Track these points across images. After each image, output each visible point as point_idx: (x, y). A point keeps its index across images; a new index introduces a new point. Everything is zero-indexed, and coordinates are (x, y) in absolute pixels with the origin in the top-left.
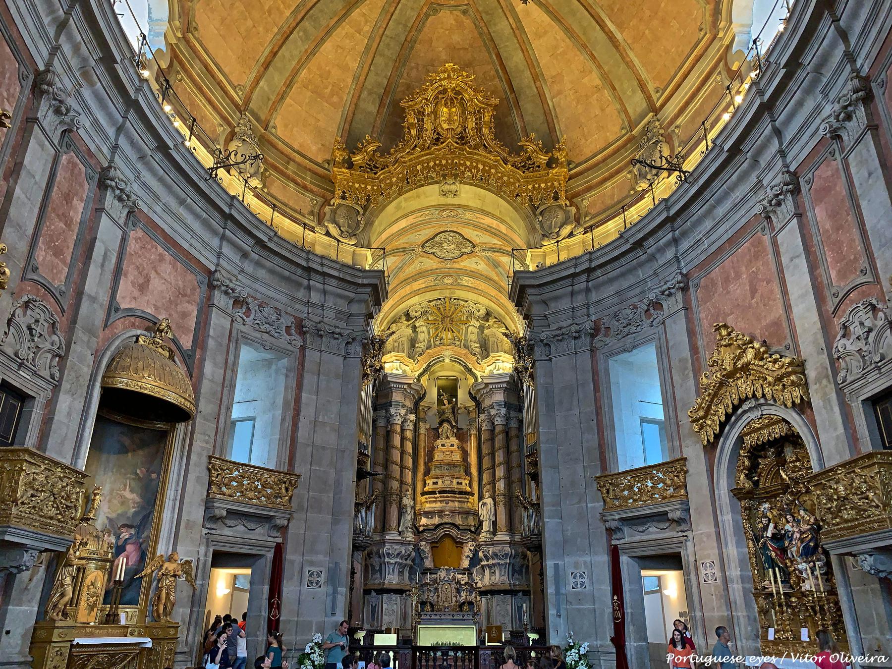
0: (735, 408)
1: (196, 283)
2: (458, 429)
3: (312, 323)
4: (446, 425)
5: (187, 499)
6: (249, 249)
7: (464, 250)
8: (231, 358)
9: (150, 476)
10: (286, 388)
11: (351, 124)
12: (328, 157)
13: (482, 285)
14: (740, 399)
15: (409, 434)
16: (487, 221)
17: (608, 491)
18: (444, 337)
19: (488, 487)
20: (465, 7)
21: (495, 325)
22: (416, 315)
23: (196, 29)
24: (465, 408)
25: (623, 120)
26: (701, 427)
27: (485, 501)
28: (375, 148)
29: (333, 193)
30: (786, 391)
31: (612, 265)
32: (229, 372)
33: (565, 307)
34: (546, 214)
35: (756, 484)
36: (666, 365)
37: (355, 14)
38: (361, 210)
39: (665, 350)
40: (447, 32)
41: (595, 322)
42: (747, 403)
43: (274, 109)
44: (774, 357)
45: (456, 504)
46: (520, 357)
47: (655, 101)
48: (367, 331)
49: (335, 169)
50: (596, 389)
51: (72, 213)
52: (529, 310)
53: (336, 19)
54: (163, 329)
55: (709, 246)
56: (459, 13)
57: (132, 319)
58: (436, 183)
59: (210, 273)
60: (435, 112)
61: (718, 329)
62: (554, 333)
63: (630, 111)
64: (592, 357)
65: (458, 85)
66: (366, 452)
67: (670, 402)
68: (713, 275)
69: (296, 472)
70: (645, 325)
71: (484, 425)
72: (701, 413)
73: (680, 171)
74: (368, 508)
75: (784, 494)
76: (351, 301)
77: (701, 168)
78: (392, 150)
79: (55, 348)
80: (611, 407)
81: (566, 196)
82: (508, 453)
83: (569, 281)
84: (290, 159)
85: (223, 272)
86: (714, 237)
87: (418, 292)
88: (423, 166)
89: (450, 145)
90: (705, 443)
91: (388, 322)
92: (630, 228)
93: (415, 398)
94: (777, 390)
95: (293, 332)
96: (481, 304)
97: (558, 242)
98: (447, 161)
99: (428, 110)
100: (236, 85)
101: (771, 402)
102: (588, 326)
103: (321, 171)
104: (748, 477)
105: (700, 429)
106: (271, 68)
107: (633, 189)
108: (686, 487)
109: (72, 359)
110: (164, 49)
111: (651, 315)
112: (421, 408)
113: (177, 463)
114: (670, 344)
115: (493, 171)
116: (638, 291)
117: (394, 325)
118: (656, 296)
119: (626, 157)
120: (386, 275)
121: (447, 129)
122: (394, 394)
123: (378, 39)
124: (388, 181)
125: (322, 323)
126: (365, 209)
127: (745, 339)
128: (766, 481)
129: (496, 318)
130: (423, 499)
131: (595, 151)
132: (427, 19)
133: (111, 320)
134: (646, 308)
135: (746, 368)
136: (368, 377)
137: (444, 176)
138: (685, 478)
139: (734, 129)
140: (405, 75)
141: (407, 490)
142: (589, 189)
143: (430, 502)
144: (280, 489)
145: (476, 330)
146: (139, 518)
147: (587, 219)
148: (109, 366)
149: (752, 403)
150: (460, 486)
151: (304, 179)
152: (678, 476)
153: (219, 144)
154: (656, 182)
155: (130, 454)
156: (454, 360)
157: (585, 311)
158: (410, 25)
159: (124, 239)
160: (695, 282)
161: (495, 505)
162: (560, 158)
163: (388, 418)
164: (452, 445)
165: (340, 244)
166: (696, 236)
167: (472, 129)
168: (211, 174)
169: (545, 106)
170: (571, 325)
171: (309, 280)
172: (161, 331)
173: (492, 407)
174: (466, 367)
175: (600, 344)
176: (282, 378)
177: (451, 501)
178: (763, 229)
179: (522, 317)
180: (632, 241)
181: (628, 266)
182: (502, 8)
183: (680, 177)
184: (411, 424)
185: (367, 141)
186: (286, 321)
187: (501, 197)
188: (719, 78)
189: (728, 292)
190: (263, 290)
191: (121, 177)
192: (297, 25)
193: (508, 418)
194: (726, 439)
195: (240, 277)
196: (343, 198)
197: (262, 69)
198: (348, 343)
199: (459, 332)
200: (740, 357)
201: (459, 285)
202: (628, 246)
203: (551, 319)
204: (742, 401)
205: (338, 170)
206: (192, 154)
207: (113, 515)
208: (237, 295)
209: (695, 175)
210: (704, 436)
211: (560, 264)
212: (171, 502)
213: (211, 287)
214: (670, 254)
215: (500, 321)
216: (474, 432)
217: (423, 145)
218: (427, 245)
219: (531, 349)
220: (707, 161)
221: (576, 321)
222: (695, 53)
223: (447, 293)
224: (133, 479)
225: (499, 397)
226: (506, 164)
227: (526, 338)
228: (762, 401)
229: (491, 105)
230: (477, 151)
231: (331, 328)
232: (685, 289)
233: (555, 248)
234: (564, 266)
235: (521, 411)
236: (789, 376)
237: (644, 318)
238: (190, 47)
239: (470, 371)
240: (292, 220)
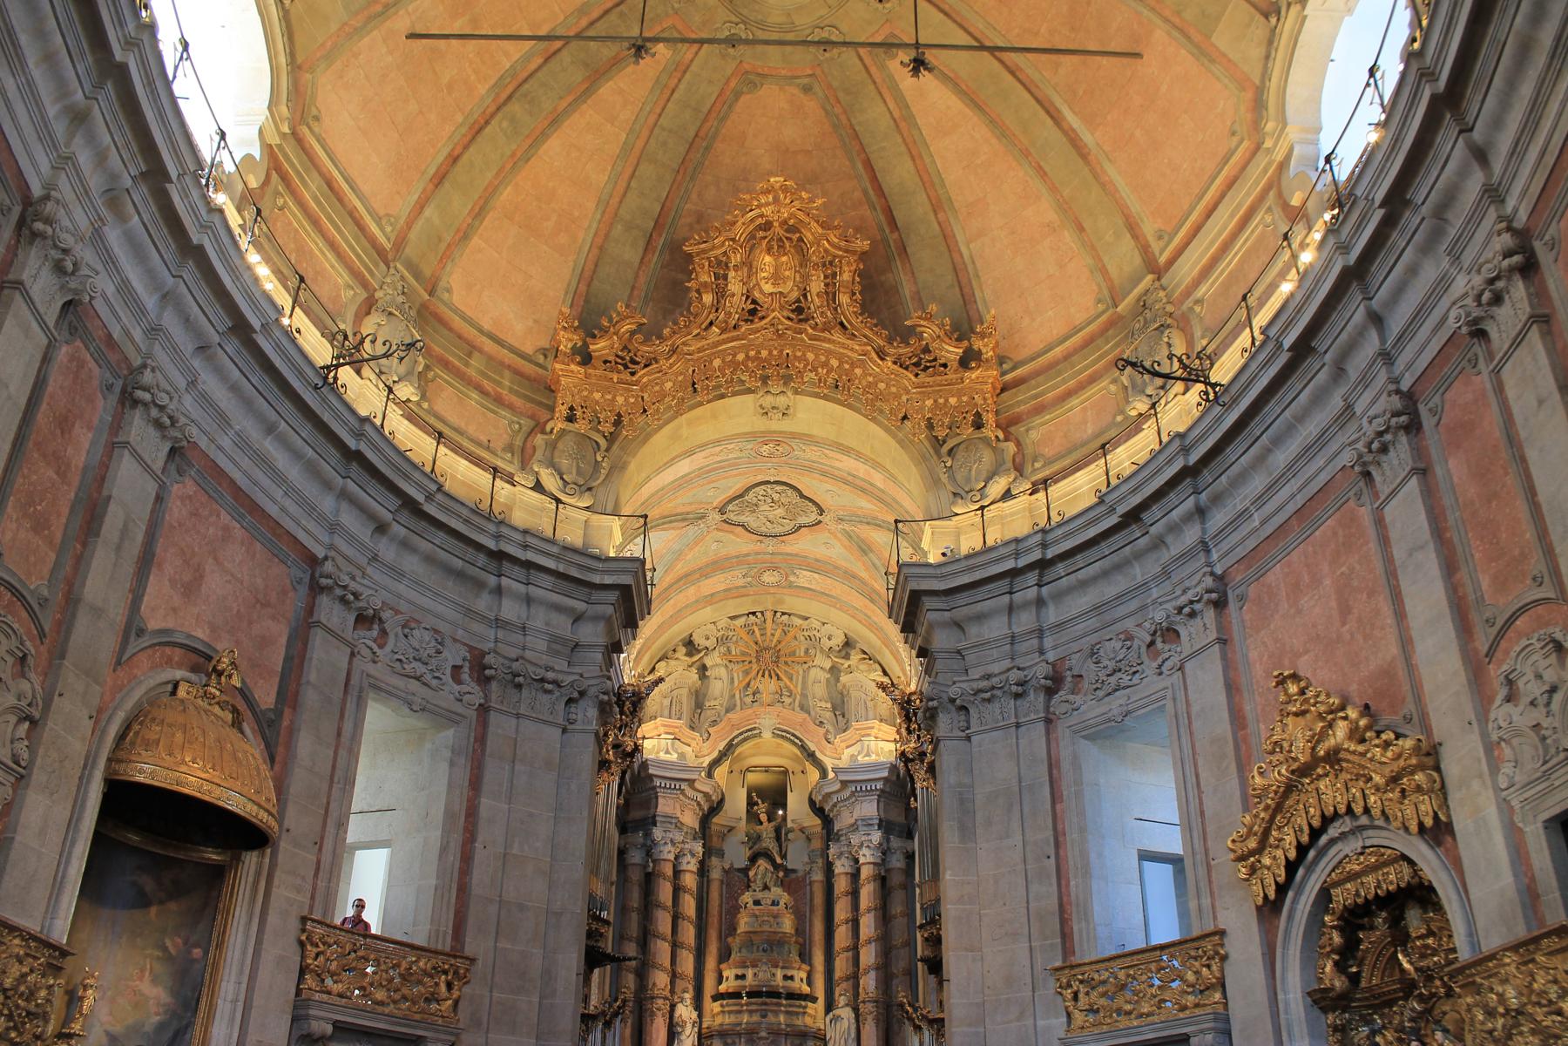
0: (1315, 834)
1: (288, 581)
2: (787, 871)
3: (501, 660)
4: (762, 863)
5: (257, 1001)
6: (388, 516)
7: (803, 520)
8: (348, 727)
9: (190, 953)
10: (450, 786)
12: (544, 342)
13: (838, 588)
14: (1323, 816)
15: (689, 880)
16: (847, 464)
17: (1076, 997)
18: (761, 687)
19: (844, 985)
20: (806, 81)
21: (862, 667)
22: (708, 643)
23: (317, 118)
24: (802, 830)
25: (1099, 285)
26: (1253, 870)
27: (836, 1012)
28: (634, 327)
29: (552, 409)
30: (1406, 802)
31: (1086, 553)
32: (343, 753)
33: (995, 634)
34: (960, 454)
35: (1355, 979)
36: (1187, 751)
37: (606, 90)
38: (603, 443)
39: (1184, 721)
41: (1054, 665)
42: (1336, 824)
43: (446, 257)
44: (1384, 736)
45: (782, 1018)
46: (909, 731)
47: (1157, 254)
48: (610, 678)
49: (558, 366)
50: (1055, 798)
51: (70, 451)
52: (927, 640)
53: (570, 99)
54: (224, 671)
55: (1263, 523)
56: (796, 91)
57: (168, 650)
58: (749, 391)
59: (313, 561)
60: (748, 264)
61: (1281, 681)
62: (975, 685)
63: (1113, 271)
64: (1048, 733)
65: (792, 216)
66: (604, 915)
67: (1194, 818)
68: (1271, 578)
69: (469, 950)
70: (1148, 672)
72: (1252, 844)
73: (1206, 383)
74: (608, 1024)
75: (1406, 998)
76: (578, 618)
77: (1243, 378)
78: (666, 331)
79: (24, 703)
80: (1082, 830)
81: (996, 421)
82: (884, 916)
83: (1003, 585)
84: (472, 348)
85: (340, 560)
86: (1269, 508)
87: (711, 599)
90: (1260, 901)
91: (651, 658)
92: (1117, 487)
93: (701, 808)
94: (1391, 800)
95: (465, 676)
96: (834, 624)
97: (982, 508)
98: (770, 353)
99: (736, 259)
100: (382, 212)
101: (1381, 822)
102: (1042, 670)
103: (529, 368)
104: (1340, 967)
105: (1251, 875)
106: (447, 184)
107: (1122, 412)
108: (1223, 986)
109: (53, 726)
110: (258, 158)
111: (1158, 654)
112: (713, 827)
113: (241, 929)
114: (1195, 709)
115: (858, 371)
116: (1133, 605)
117: (662, 664)
118: (1168, 616)
119: (1107, 353)
120: (648, 566)
121: (771, 294)
122: (661, 801)
123: (645, 133)
124: (657, 388)
125: (521, 661)
126: (611, 438)
127: (1331, 701)
128: (1372, 975)
129: (865, 653)
130: (716, 1007)
133: (130, 651)
134: (1148, 639)
135: (1333, 757)
136: (610, 768)
137: (765, 380)
138: (1222, 970)
139: (1299, 310)
140: (694, 196)
142: (1040, 410)
143: (730, 1012)
144: (437, 984)
145: (824, 676)
146: (169, 1034)
147: (1037, 465)
148: (122, 737)
149: (1345, 825)
151: (499, 384)
152: (1208, 966)
153: (344, 322)
154: (1163, 401)
155: (153, 910)
156: (781, 734)
157: (1035, 642)
158: (705, 110)
159: (159, 499)
160: (1238, 591)
161: (857, 1021)
162: (984, 351)
163: (649, 849)
164: (774, 903)
165: (561, 506)
166: (1237, 503)
167: (818, 295)
168: (325, 379)
170: (1009, 670)
171: (499, 576)
172: (220, 674)
173: (854, 827)
174: (803, 748)
175: (1064, 707)
176: (444, 766)
177: (772, 1011)
178: (1359, 496)
179: (914, 653)
180: (1122, 509)
181: (1115, 558)
182: (874, 82)
183: (1206, 393)
184: (693, 861)
185: (618, 314)
186: (454, 655)
187: (874, 420)
188: (1268, 219)
189: (1299, 612)
190: (413, 595)
191: (164, 385)
192: (498, 109)
193: (885, 851)
194: (1298, 893)
195: (369, 570)
196: (571, 419)
197: (431, 186)
198: (570, 701)
199: (791, 679)
200: (1322, 736)
201: (791, 586)
202: (1113, 520)
203: (971, 658)
204: (1327, 821)
205: (563, 367)
206: (293, 341)
207: (117, 1029)
208: (361, 604)
209: (1233, 390)
210: (1257, 889)
211: (987, 550)
212: (228, 1005)
213: (316, 589)
214: (1191, 535)
215: (868, 656)
216: (818, 876)
217: (726, 322)
218: (730, 507)
219: (932, 715)
220: (1254, 366)
221: (1020, 662)
222: (1224, 173)
223: (768, 604)
224: (158, 958)
225: (869, 808)
226: (882, 359)
227: (921, 693)
228: (1364, 820)
229: (854, 253)
230: (826, 335)
231: (538, 671)
232: (1220, 605)
233: (978, 519)
234: (994, 555)
235: (910, 836)
236: (1412, 773)
237: (1144, 657)
238: (303, 149)
239: (811, 756)
240: (471, 461)
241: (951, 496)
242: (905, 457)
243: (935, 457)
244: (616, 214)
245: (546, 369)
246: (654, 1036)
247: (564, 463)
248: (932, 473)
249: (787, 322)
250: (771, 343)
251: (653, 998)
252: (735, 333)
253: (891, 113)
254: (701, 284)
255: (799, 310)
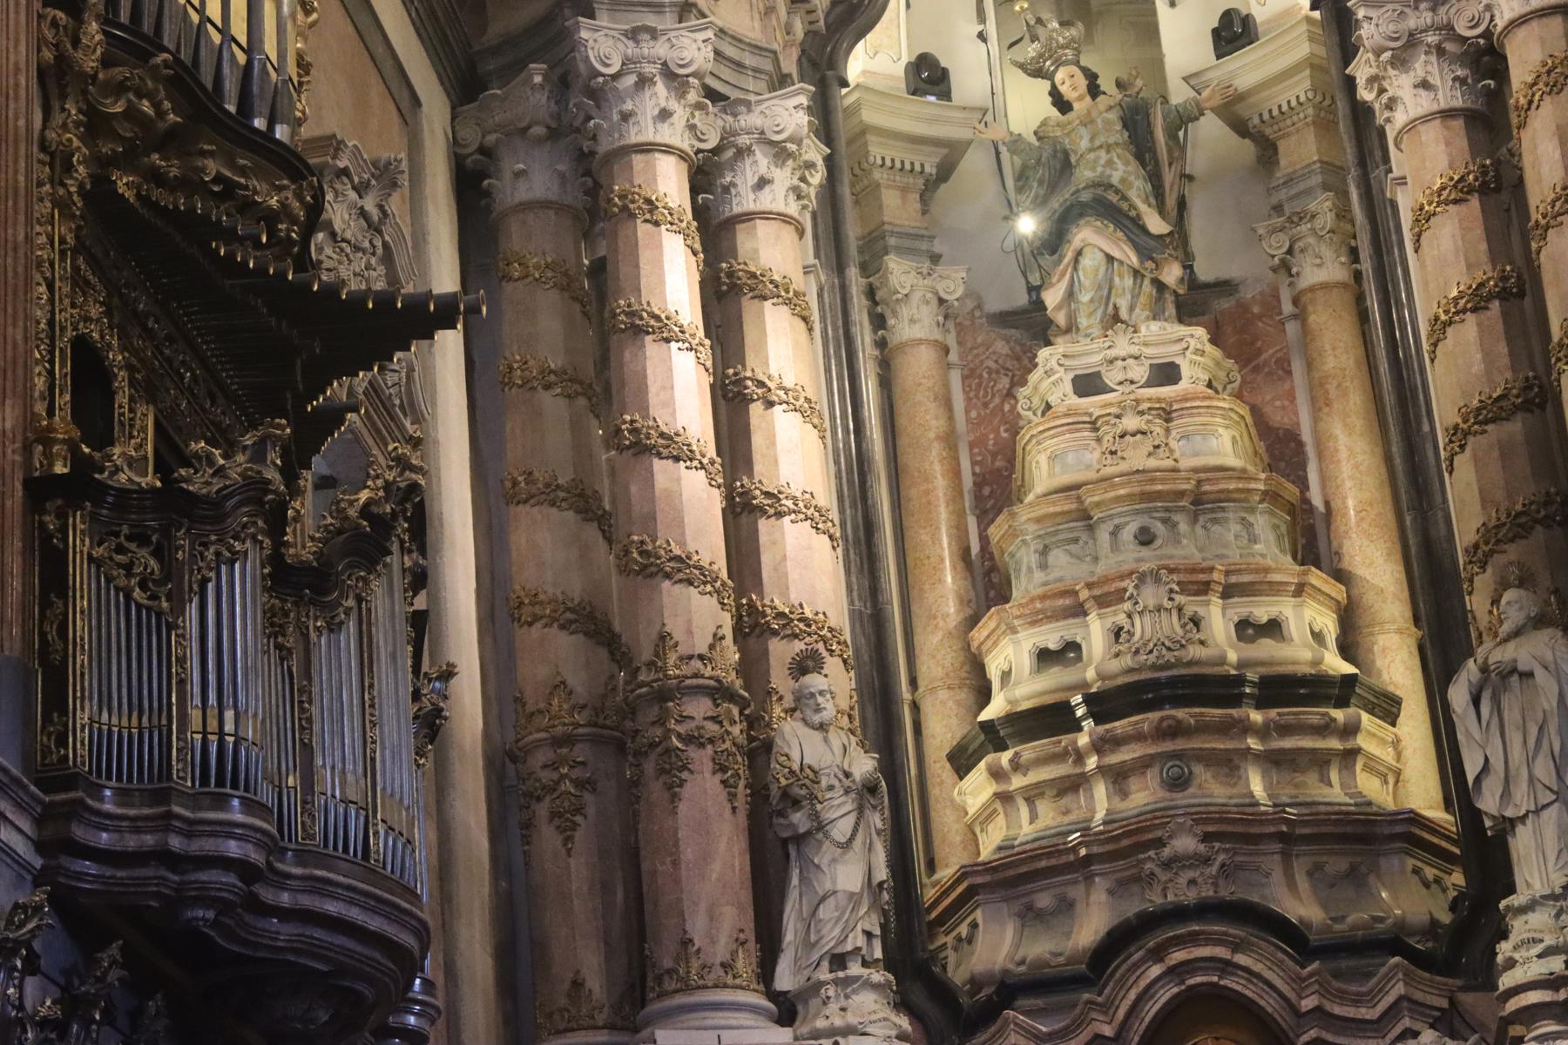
24: (1235, 113)
71: (1401, 84)
112: (877, 150)
130: (976, 789)
141: (805, 665)
143: (1032, 795)
150: (1266, 648)
164: (1167, 373)
184: (783, 178)
246: (688, 853)
251: (663, 696)
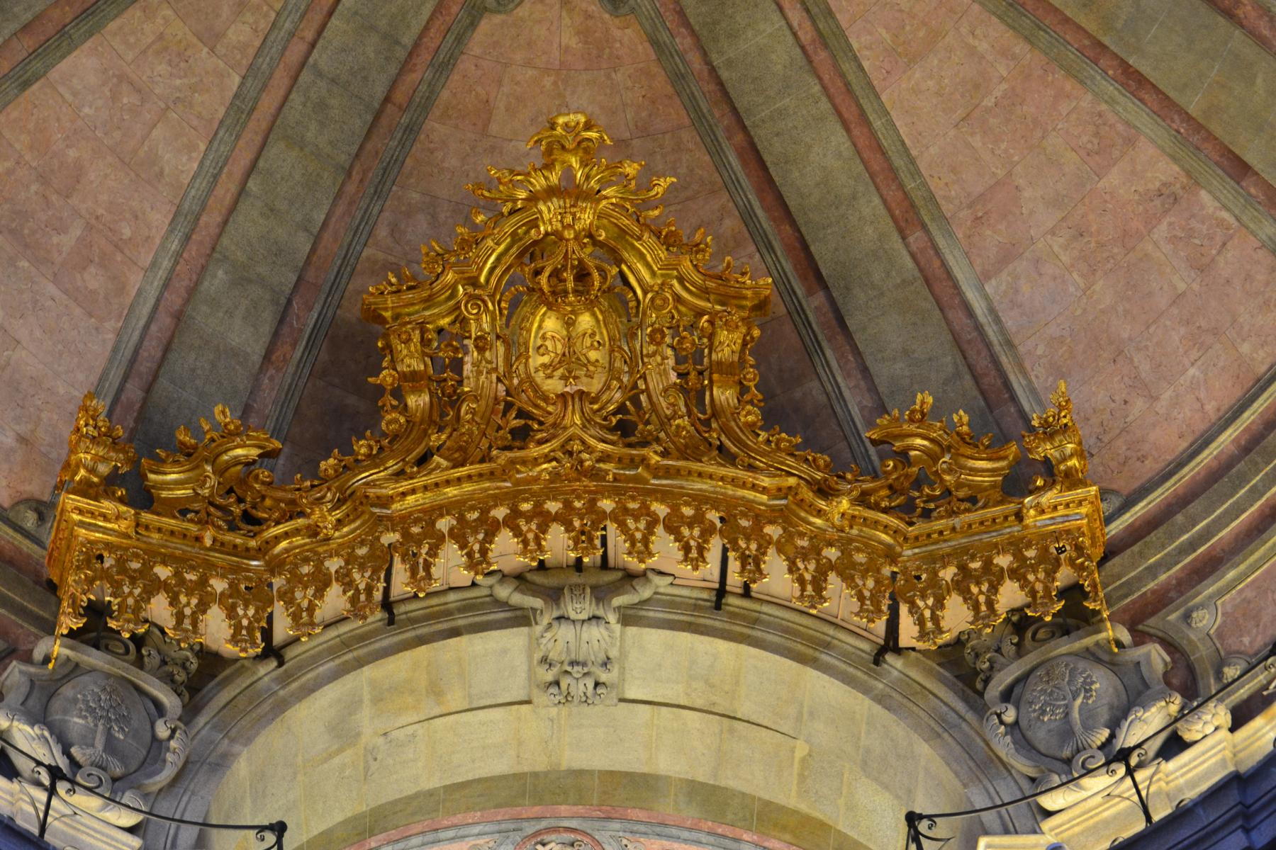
11: (155, 377)
12: (37, 487)
28: (254, 452)
40: (548, 82)
58: (522, 618)
88: (461, 519)
89: (577, 446)
98: (568, 505)
121: (563, 396)
123: (280, 81)
124: (305, 569)
131: (1201, 426)
132: (473, 25)
140: (382, 232)
147: (1230, 672)
158: (408, 40)
169: (958, 317)
205: (83, 503)
211: (1155, 831)
230: (695, 466)
241: (1026, 785)
242: (899, 729)
243: (970, 716)
244: (213, 249)
245: (38, 542)
247: (77, 723)
248: (967, 748)
249: (601, 446)
250: (566, 486)
252: (485, 467)
253: (795, 34)
254: (404, 377)
255: (624, 429)
